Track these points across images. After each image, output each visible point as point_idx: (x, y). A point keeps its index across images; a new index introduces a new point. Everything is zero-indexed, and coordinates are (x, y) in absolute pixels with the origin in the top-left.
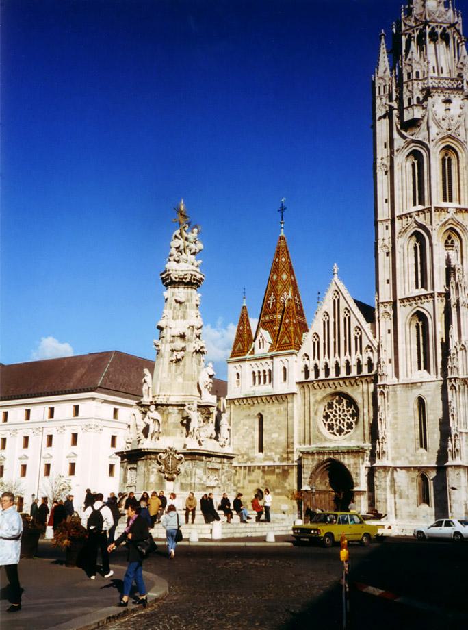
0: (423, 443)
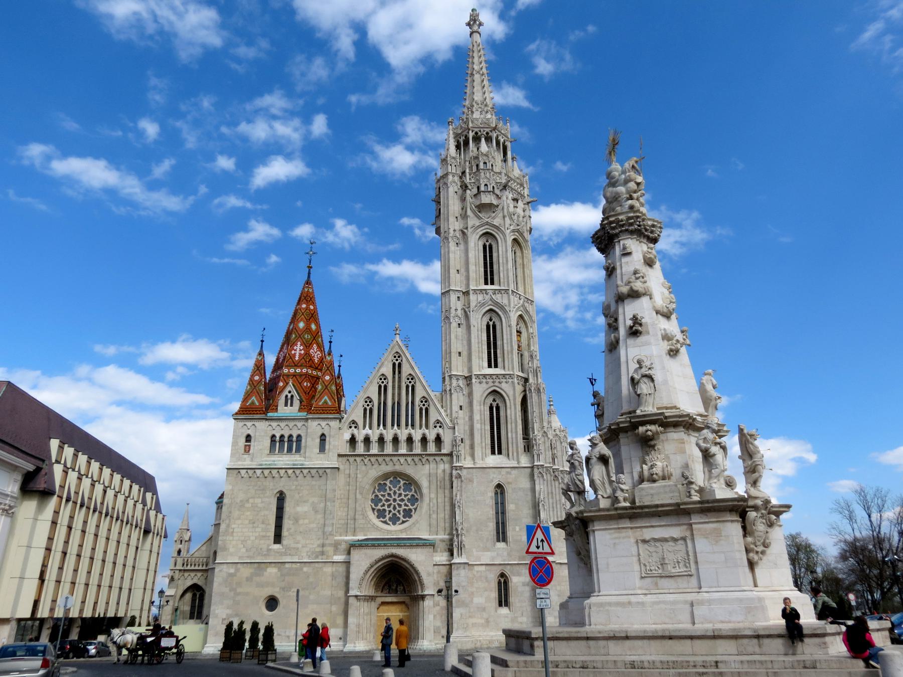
0: (501, 535)
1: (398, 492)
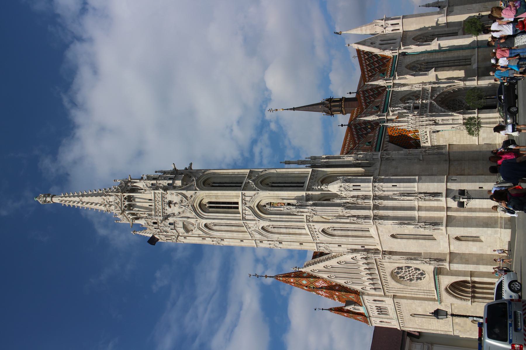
1: (403, 272)
